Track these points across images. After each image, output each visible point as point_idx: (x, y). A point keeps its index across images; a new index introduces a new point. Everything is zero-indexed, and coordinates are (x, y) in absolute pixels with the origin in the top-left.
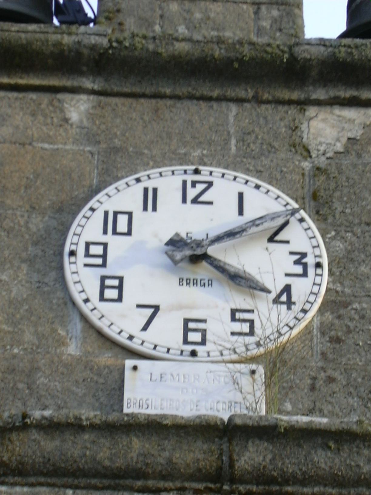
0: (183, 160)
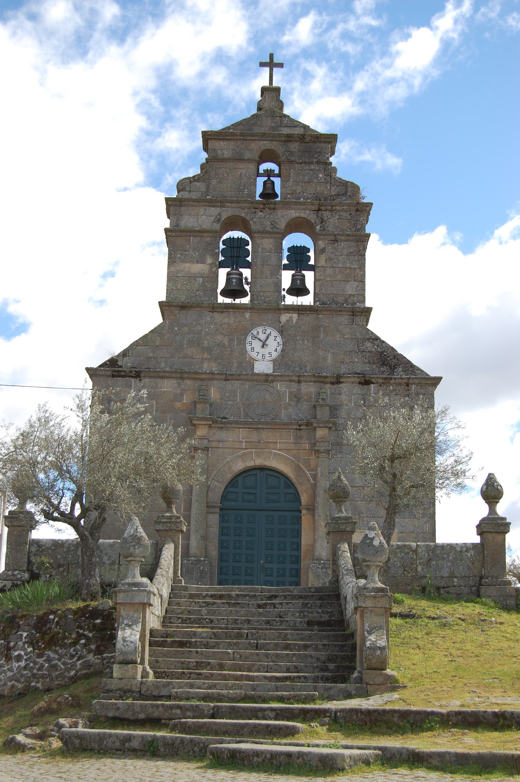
0: (263, 325)
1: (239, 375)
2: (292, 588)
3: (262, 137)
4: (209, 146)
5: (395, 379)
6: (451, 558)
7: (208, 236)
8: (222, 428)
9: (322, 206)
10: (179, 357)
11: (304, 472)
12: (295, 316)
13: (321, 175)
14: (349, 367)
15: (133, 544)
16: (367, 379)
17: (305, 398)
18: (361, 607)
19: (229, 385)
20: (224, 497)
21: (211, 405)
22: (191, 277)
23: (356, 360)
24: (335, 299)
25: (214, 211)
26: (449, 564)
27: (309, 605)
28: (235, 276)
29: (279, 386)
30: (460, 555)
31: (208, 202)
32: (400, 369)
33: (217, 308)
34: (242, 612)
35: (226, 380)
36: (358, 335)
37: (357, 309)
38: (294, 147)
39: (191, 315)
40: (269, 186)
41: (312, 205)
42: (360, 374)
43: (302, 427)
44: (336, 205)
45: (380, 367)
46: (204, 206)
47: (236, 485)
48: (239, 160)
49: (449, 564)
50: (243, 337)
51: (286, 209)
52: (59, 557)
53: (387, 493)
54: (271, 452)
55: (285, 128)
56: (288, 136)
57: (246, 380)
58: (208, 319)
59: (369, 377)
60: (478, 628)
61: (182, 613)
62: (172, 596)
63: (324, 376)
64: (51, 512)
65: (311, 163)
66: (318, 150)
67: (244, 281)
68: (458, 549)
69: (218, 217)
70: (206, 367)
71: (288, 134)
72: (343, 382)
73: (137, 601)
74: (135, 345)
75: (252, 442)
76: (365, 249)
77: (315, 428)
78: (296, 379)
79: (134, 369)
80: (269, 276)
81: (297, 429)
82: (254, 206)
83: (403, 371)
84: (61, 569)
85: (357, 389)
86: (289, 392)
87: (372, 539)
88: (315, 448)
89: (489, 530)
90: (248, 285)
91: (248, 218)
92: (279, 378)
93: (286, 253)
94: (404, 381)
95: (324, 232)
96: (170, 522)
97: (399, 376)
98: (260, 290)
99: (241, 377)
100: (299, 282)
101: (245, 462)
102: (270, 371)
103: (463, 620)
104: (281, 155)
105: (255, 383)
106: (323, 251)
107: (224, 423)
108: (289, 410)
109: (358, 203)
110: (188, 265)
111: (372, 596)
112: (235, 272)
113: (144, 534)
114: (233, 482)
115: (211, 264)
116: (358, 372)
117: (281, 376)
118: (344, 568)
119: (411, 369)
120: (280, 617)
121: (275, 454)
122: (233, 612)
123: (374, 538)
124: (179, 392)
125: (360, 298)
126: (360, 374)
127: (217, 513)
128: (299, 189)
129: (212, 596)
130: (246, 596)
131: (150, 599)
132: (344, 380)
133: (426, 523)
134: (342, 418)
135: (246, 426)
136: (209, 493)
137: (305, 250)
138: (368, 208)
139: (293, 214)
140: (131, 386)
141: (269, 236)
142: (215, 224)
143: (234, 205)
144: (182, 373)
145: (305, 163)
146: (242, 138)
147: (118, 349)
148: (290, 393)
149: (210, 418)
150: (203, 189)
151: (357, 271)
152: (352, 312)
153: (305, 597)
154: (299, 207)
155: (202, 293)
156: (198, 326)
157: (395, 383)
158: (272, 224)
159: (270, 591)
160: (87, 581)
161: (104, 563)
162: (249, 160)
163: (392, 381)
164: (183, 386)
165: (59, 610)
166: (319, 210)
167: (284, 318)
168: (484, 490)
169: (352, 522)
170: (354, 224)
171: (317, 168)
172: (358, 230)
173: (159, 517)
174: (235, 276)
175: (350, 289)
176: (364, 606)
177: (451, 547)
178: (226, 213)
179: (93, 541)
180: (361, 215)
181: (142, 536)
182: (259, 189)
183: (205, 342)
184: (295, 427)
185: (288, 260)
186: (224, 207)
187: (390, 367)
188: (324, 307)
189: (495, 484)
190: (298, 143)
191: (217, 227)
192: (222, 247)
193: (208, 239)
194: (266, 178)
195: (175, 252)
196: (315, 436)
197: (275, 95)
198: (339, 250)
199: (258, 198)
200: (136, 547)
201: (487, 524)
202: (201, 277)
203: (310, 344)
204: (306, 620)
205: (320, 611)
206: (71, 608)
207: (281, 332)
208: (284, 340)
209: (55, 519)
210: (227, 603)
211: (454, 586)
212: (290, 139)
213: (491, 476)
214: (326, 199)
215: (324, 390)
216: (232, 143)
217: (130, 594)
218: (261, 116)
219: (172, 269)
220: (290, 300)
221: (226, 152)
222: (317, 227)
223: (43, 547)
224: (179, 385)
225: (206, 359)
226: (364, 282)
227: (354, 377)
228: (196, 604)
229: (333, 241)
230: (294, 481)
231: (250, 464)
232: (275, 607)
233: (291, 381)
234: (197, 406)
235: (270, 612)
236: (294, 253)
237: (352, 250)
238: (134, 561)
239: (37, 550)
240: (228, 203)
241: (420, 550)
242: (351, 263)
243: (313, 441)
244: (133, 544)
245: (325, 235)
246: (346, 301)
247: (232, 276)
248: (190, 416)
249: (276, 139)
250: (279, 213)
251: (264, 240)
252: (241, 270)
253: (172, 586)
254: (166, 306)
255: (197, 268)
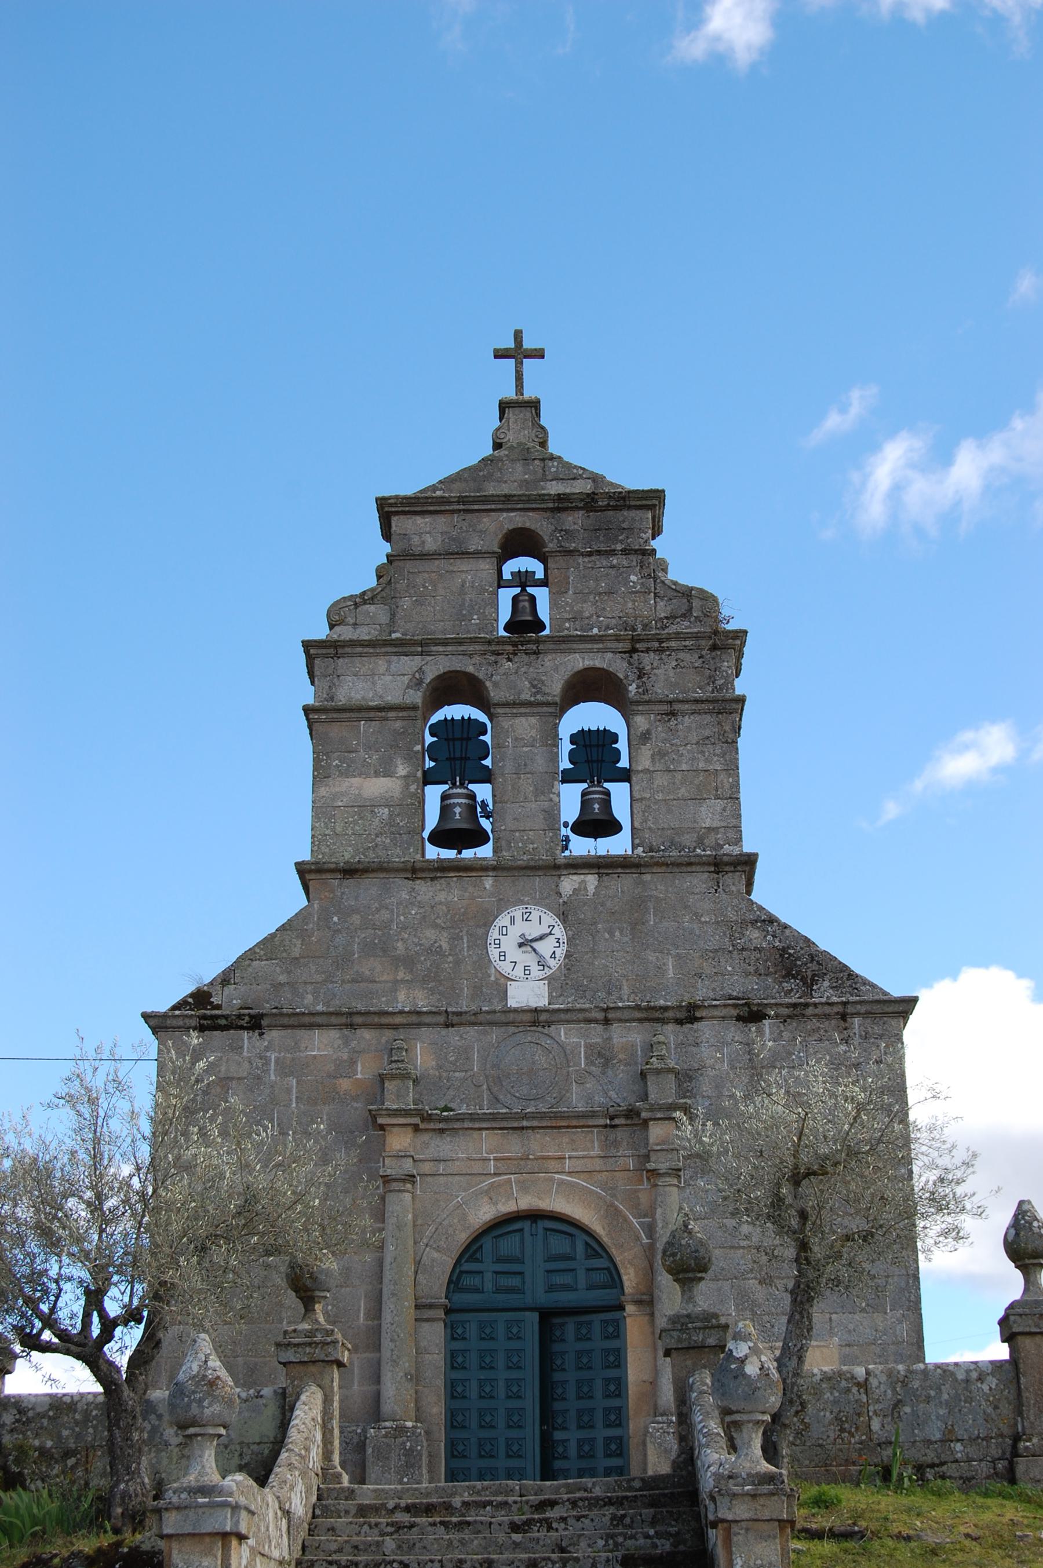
0: (522, 903)
1: (474, 1014)
2: (588, 1481)
3: (504, 502)
4: (394, 528)
5: (815, 1005)
6: (945, 1397)
7: (397, 718)
8: (442, 1131)
9: (639, 641)
10: (343, 981)
11: (626, 1219)
12: (591, 881)
13: (633, 578)
14: (714, 985)
15: (198, 1396)
16: (755, 1009)
17: (621, 1056)
18: (723, 1521)
19: (453, 1037)
20: (454, 1283)
21: (416, 1081)
22: (365, 807)
23: (730, 969)
24: (677, 839)
25: (409, 664)
26: (941, 1412)
27: (628, 1521)
28: (460, 801)
29: (563, 1033)
30: (966, 1389)
31: (395, 646)
32: (826, 984)
33: (422, 870)
34: (476, 1542)
35: (448, 1025)
36: (732, 915)
37: (726, 859)
38: (574, 521)
39: (368, 889)
40: (524, 604)
41: (618, 640)
42: (738, 999)
43: (617, 1121)
44: (668, 639)
45: (781, 983)
46: (386, 654)
47: (478, 1255)
48: (457, 553)
49: (941, 1412)
50: (480, 931)
51: (563, 651)
52: (65, 1433)
53: (790, 1253)
54: (552, 1180)
55: (554, 482)
56: (560, 498)
57: (491, 1024)
58: (405, 895)
59: (759, 1005)
60: (1010, 1557)
61: (340, 1551)
62: (318, 1512)
63: (661, 1008)
64: (35, 1331)
65: (612, 553)
66: (624, 525)
67: (479, 809)
68: (961, 1376)
69: (417, 675)
70: (403, 1000)
71: (559, 495)
72: (702, 1018)
73: (209, 1530)
74: (249, 956)
75: (509, 1159)
76: (737, 730)
77: (646, 1122)
78: (600, 1016)
79: (246, 1011)
80: (531, 797)
81: (606, 1126)
82: (493, 647)
83: (832, 988)
84: (71, 1462)
85: (734, 1032)
86: (586, 1046)
87: (742, 1361)
88: (651, 1166)
89: (1027, 1329)
90: (488, 818)
91: (481, 676)
92: (563, 1016)
93: (566, 747)
94: (836, 1009)
95: (646, 697)
96: (310, 1344)
97: (824, 1000)
98: (513, 828)
99: (481, 1018)
100: (596, 806)
101: (496, 1204)
102: (543, 1002)
103: (976, 1539)
104: (546, 538)
105: (512, 1029)
106: (645, 737)
107: (447, 1120)
108: (588, 1085)
109: (716, 633)
110: (356, 781)
111: (747, 1494)
112: (459, 791)
113: (223, 1373)
114: (472, 1250)
115: (406, 777)
116: (735, 994)
117: (567, 1011)
118: (701, 1430)
119: (849, 983)
120: (563, 1550)
121: (562, 1183)
122: (456, 1543)
123: (746, 1357)
124: (345, 1056)
125: (731, 834)
126: (738, 999)
127: (440, 1319)
128: (588, 609)
129: (408, 1509)
130: (484, 1505)
131: (238, 1522)
132: (704, 1014)
133: (901, 1322)
134: (703, 1097)
135: (495, 1125)
136: (420, 1276)
137: (608, 737)
138: (738, 642)
139: (579, 661)
140: (242, 1047)
141: (528, 710)
142: (412, 692)
143: (449, 648)
144: (351, 1014)
145: (599, 552)
146: (462, 507)
147: (209, 972)
148: (588, 1046)
149: (415, 1110)
150: (383, 618)
151: (722, 776)
152: (716, 865)
153: (619, 1502)
154: (589, 646)
155: (388, 841)
156: (383, 912)
157: (815, 1015)
158: (534, 686)
159: (540, 1491)
160: (122, 1486)
161: (167, 1444)
162: (478, 554)
163: (810, 1011)
164: (353, 1044)
165: (56, 1555)
166: (634, 650)
167: (568, 884)
168: (1010, 1238)
169: (719, 1326)
170: (710, 677)
171: (625, 563)
172: (720, 689)
173: (286, 1332)
174: (460, 801)
175: (708, 815)
176: (730, 1517)
177: (944, 1371)
178: (435, 667)
179: (132, 1395)
180: (723, 657)
181: (218, 1378)
182: (505, 614)
183: (400, 944)
184: (602, 1122)
185: (571, 762)
186: (429, 654)
187: (803, 980)
188: (652, 857)
189: (1035, 1224)
190: (581, 512)
191: (417, 697)
192: (429, 739)
193: (398, 724)
194: (518, 590)
195: (327, 754)
196: (647, 1139)
197: (528, 415)
198: (680, 733)
199: (502, 633)
200: (206, 1404)
201: (1021, 1315)
202: (386, 806)
203: (627, 939)
204: (619, 1554)
205: (652, 1532)
206: (80, 1552)
207: (563, 916)
208: (570, 933)
209: (46, 1348)
210: (442, 1523)
211: (956, 1461)
212: (566, 505)
213: (1025, 1207)
214: (645, 626)
215: (661, 1038)
216: (441, 519)
217: (191, 1513)
218: (500, 459)
219: (323, 791)
220: (581, 846)
221: (428, 538)
222: (630, 688)
223: (30, 1414)
224: (346, 1043)
225: (402, 981)
226: (738, 799)
227: (725, 1006)
228: (371, 1528)
229: (667, 714)
230: (605, 1239)
231: (508, 1207)
232: (550, 1528)
233: (589, 1021)
234: (386, 1085)
235: (538, 1540)
236: (585, 746)
237: (707, 733)
238: (200, 1435)
239: (17, 1421)
240: (436, 645)
241: (874, 1382)
242: (707, 761)
243: (643, 1151)
244: (198, 1396)
245: (648, 702)
246: (700, 842)
247: (452, 801)
248: (371, 1107)
249: (534, 506)
250: (548, 661)
251: (517, 721)
252: (471, 786)
253: (319, 1489)
254: (310, 871)
255: (376, 787)
